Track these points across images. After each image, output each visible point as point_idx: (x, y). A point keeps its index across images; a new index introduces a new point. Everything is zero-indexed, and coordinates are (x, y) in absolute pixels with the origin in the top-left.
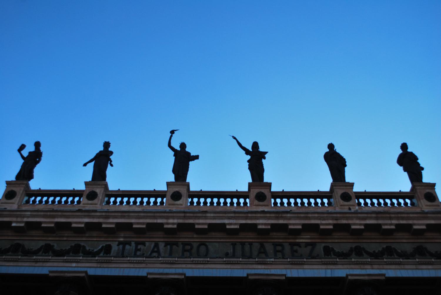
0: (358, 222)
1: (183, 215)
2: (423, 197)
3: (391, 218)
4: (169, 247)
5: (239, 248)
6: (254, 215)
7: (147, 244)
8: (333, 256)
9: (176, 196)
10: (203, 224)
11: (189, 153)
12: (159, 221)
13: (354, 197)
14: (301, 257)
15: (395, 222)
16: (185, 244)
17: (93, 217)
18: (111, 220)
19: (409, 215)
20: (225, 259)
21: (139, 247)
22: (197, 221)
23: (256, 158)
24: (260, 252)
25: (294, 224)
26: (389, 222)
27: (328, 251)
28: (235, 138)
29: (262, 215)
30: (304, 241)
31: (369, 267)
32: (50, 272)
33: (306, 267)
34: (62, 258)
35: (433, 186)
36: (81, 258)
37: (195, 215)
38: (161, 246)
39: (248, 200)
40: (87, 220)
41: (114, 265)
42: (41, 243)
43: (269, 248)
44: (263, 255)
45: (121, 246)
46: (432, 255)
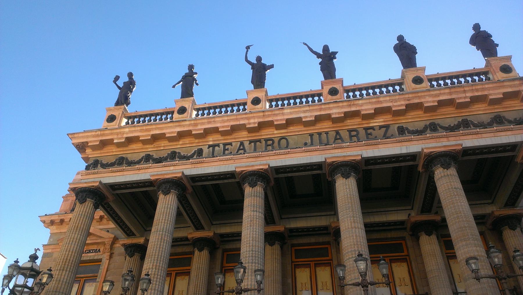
0: (430, 99)
1: (262, 114)
2: (499, 70)
4: (253, 144)
5: (316, 137)
6: (327, 106)
7: (234, 144)
8: (407, 134)
9: (256, 101)
10: (281, 120)
11: (264, 65)
12: (242, 122)
13: (427, 80)
14: (376, 138)
16: (266, 140)
17: (184, 126)
18: (199, 127)
19: (484, 87)
20: (304, 149)
21: (227, 147)
22: (275, 118)
23: (327, 60)
24: (336, 139)
25: (366, 110)
26: (464, 95)
27: (402, 131)
28: (306, 44)
29: (335, 105)
30: (377, 124)
31: (445, 139)
32: (151, 176)
33: (380, 146)
34: (161, 164)
35: (509, 58)
36: (177, 162)
37: (273, 113)
38: (246, 144)
39: (321, 98)
40: (179, 129)
42: (143, 155)
43: (345, 135)
44: (340, 141)
45: (211, 148)
46: (510, 122)
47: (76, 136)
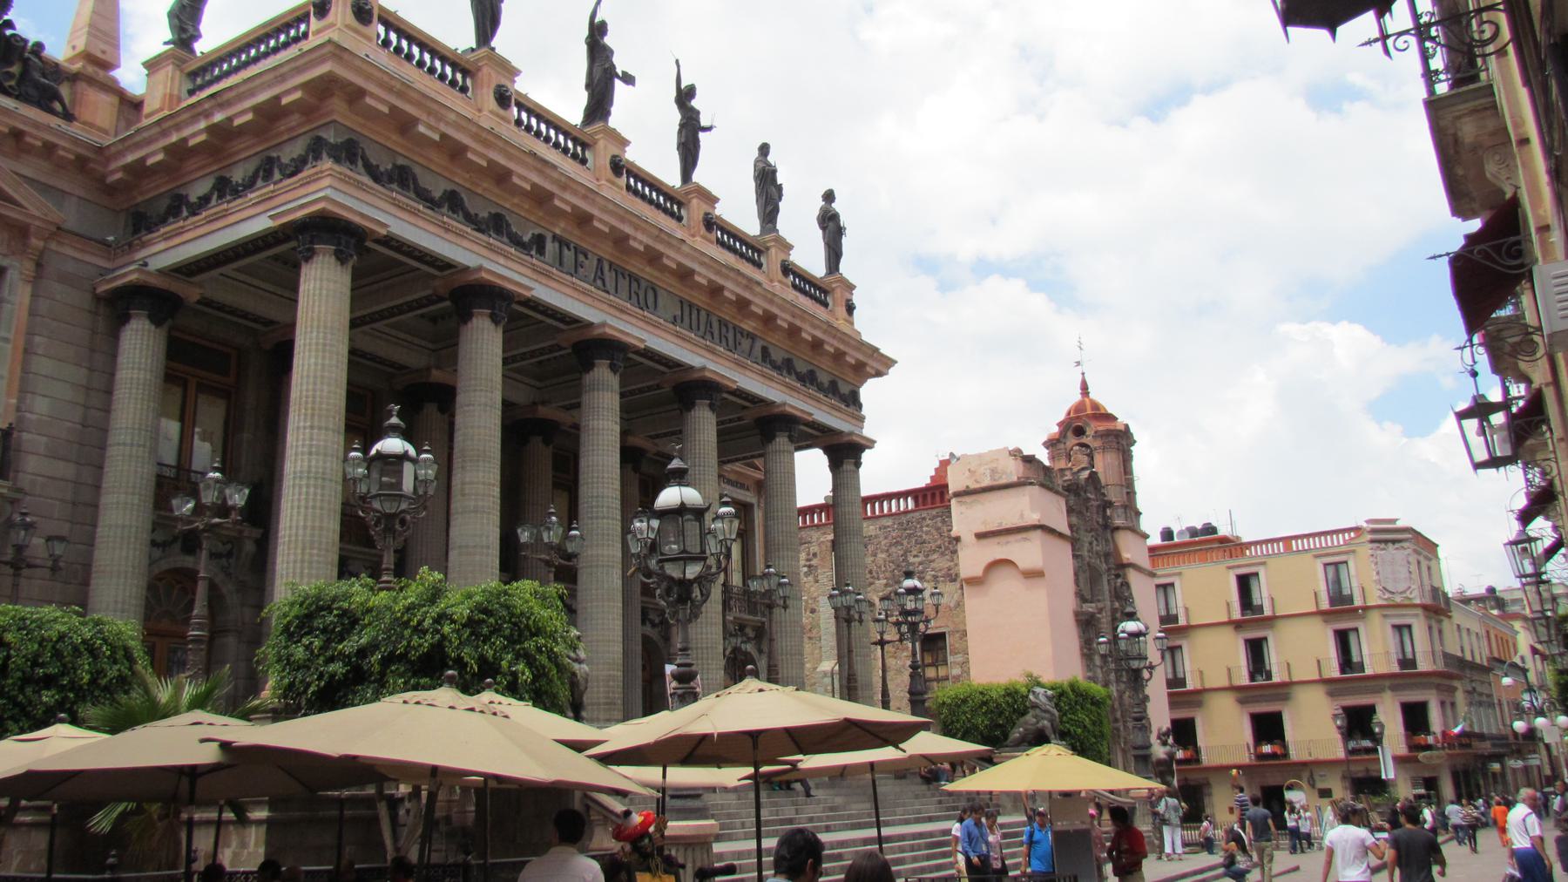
3: (834, 337)
15: (836, 343)
18: (568, 196)
41: (554, 284)
47: (346, 56)
